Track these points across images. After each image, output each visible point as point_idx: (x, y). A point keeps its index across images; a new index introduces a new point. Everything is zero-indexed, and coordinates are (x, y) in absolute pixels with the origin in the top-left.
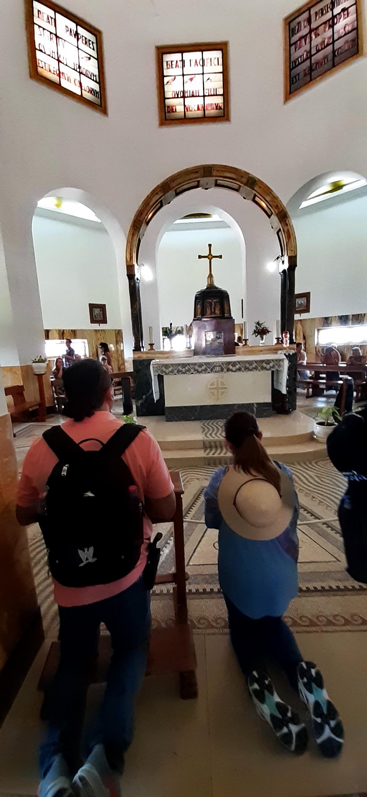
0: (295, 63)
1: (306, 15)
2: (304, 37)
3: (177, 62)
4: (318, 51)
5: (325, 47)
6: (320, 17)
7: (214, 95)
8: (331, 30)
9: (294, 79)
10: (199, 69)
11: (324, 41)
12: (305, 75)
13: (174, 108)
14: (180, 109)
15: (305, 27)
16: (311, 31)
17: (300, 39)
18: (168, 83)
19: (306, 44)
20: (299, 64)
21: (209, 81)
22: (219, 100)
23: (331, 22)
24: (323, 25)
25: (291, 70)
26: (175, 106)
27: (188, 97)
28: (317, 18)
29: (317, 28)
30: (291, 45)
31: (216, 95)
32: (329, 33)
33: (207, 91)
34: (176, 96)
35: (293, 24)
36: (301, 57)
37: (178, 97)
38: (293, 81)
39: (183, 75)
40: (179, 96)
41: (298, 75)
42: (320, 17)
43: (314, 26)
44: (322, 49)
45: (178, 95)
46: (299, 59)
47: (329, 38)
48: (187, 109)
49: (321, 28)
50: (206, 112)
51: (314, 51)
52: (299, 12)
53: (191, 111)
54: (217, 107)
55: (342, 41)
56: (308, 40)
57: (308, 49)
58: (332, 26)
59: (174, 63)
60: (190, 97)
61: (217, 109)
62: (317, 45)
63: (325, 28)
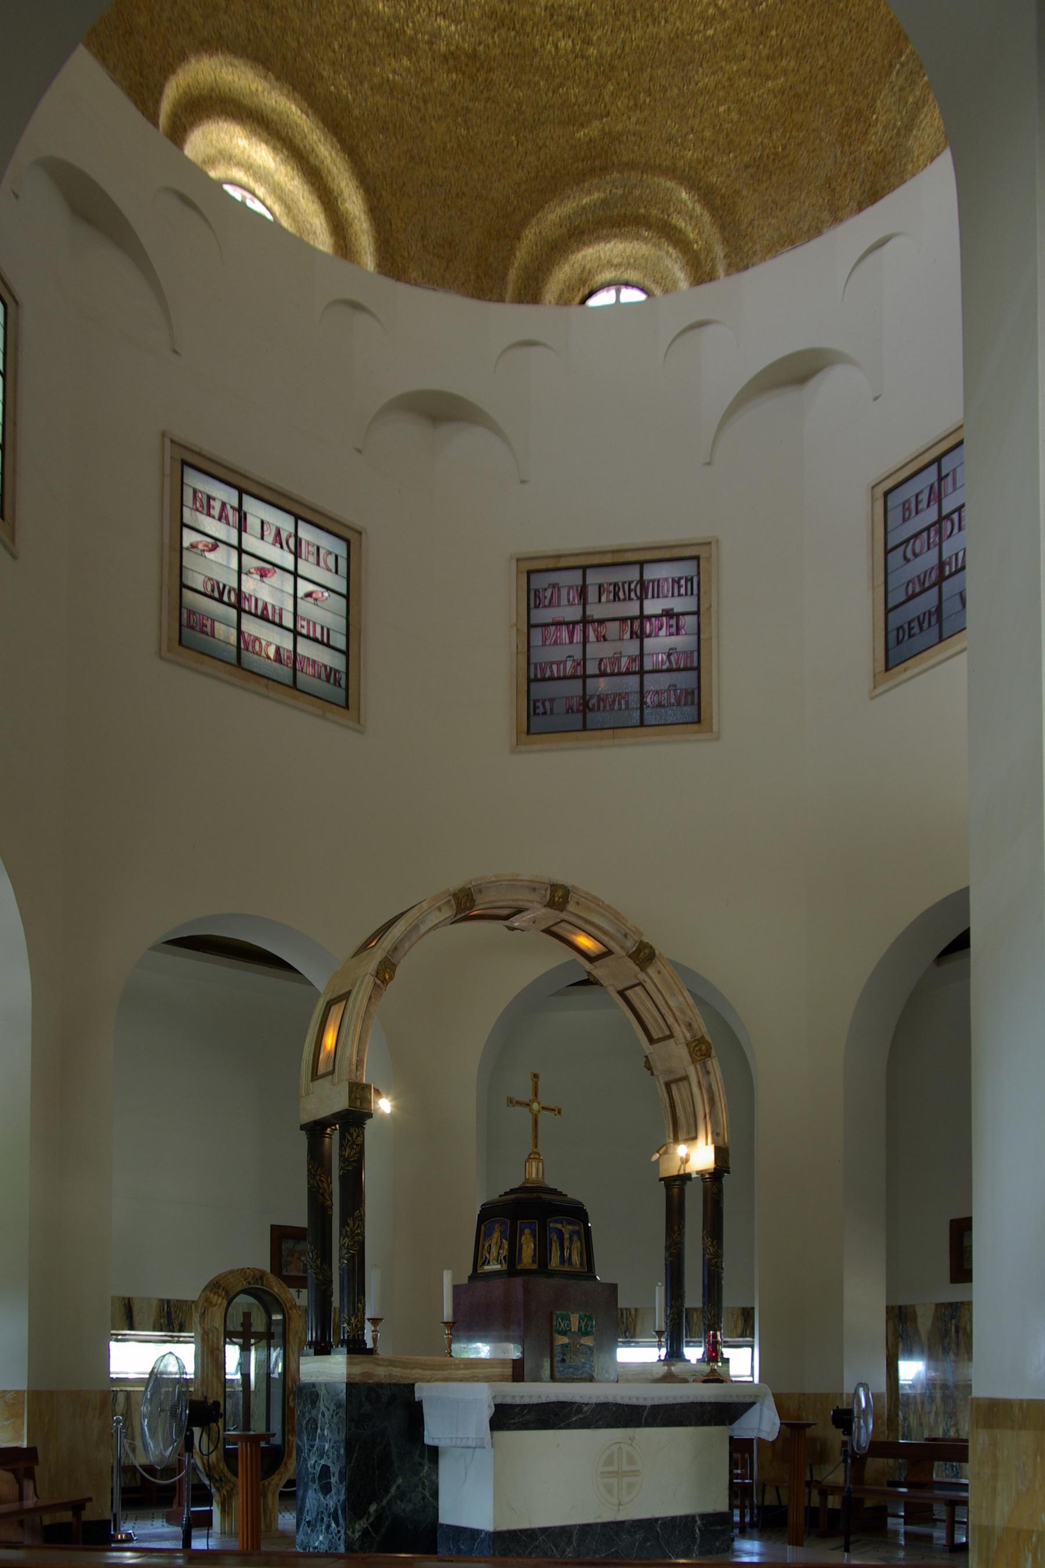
0: (543, 671)
1: (575, 578)
2: (571, 624)
3: (224, 505)
4: (603, 674)
5: (620, 674)
6: (608, 601)
7: (322, 643)
8: (637, 642)
9: (539, 704)
10: (288, 561)
11: (619, 659)
12: (570, 710)
13: (208, 623)
14: (226, 633)
15: (570, 604)
16: (585, 621)
17: (558, 624)
18: (193, 546)
19: (571, 642)
20: (552, 679)
21: (309, 599)
22: (336, 661)
23: (638, 627)
24: (617, 623)
25: (529, 681)
26: (213, 621)
27: (250, 613)
28: (604, 598)
29: (601, 622)
30: (530, 626)
31: (328, 645)
32: (632, 648)
33: (305, 623)
34: (216, 595)
35: (541, 581)
36: (558, 664)
37: (220, 600)
38: (535, 708)
39: (241, 551)
40: (225, 598)
41: (552, 701)
42: (608, 601)
43: (595, 611)
44: (612, 674)
45: (221, 594)
46: (555, 667)
47: (632, 659)
48: (246, 644)
49: (613, 628)
50: (299, 674)
51: (592, 668)
52: (556, 565)
53: (258, 654)
54: (330, 674)
55: (663, 681)
56: (578, 637)
57: (579, 656)
58: (640, 636)
59: (217, 506)
60: (256, 615)
61: (328, 680)
62: (601, 660)
63: (622, 631)
